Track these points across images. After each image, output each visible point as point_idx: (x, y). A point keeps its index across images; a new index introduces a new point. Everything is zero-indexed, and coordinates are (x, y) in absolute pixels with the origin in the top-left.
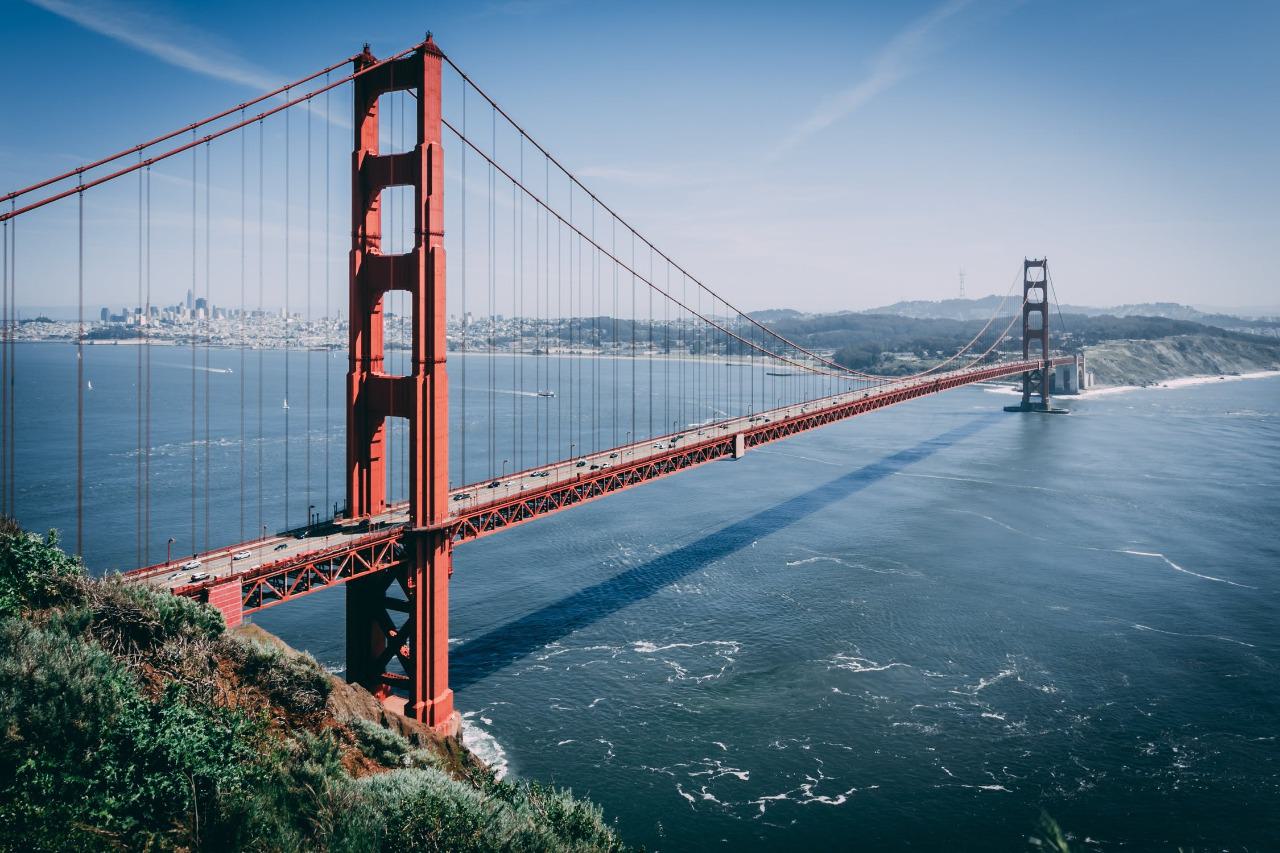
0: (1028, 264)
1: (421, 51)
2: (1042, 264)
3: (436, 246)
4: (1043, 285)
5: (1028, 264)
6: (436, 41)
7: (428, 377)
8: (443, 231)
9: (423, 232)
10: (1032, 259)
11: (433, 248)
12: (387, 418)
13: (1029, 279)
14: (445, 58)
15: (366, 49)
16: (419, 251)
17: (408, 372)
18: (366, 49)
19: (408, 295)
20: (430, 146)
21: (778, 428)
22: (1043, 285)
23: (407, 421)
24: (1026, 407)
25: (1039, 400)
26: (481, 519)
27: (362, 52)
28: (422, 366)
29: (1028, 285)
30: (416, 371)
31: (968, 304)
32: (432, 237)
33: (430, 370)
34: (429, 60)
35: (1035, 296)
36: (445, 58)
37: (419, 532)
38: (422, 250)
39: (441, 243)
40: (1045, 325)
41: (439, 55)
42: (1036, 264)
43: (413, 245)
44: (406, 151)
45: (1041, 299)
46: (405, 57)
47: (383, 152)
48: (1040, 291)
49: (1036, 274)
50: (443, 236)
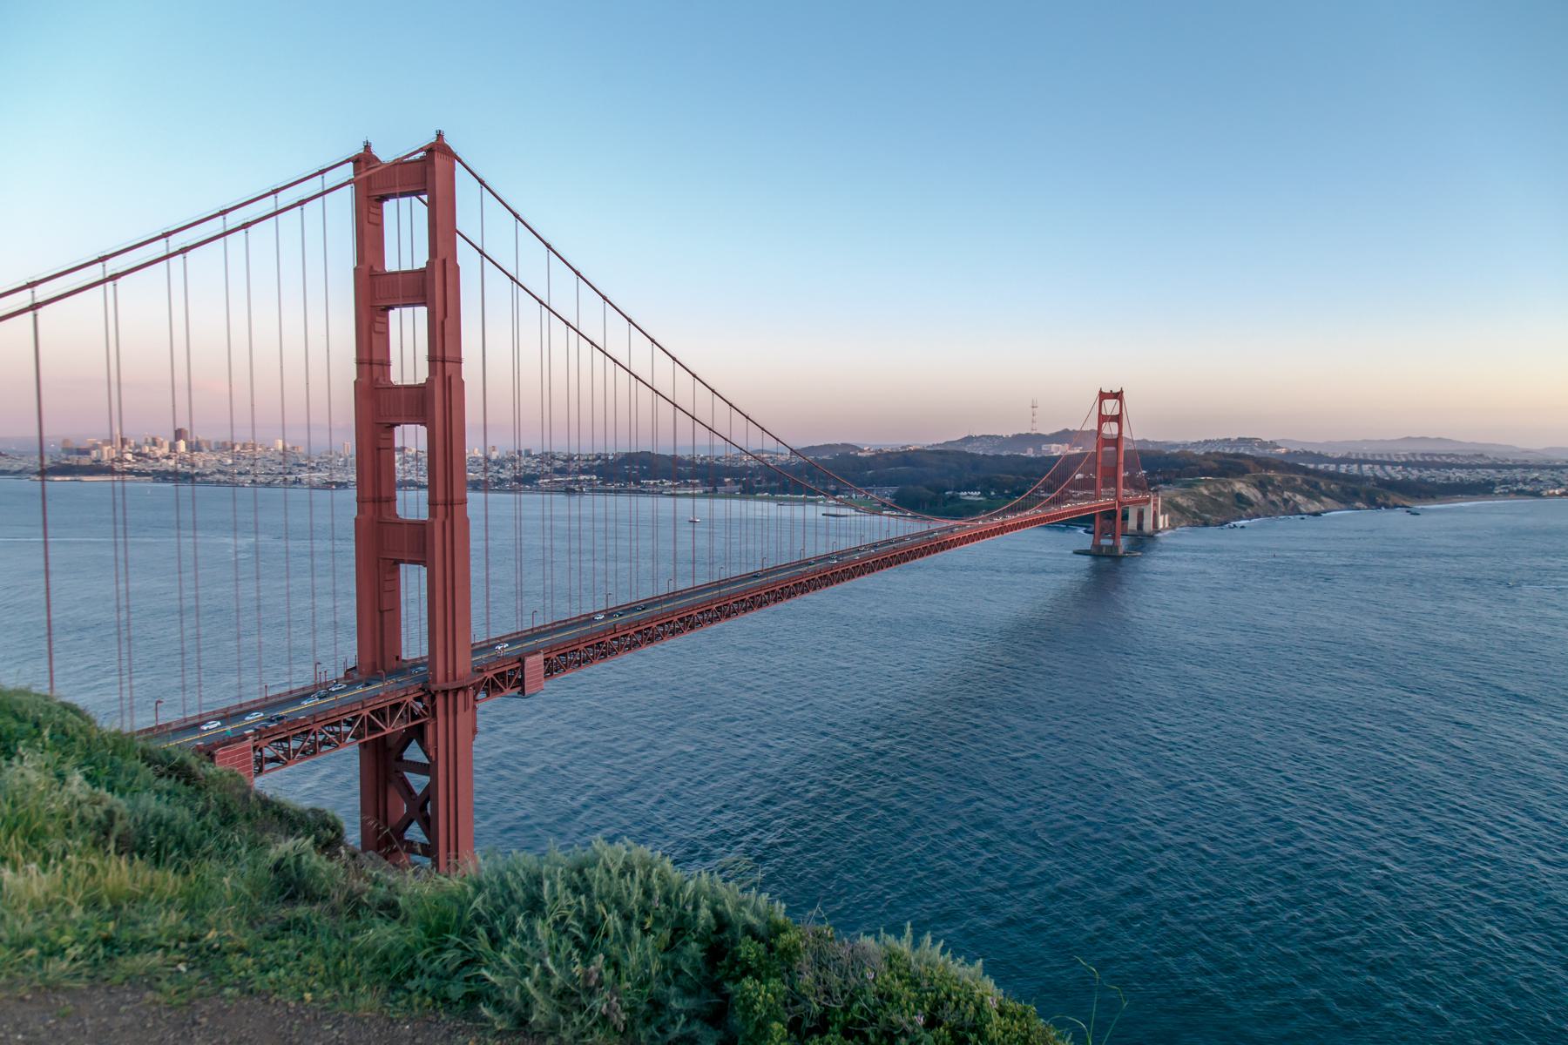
1: (430, 150)
2: (1118, 396)
4: (1117, 419)
5: (1103, 396)
6: (449, 140)
8: (460, 359)
10: (1106, 390)
11: (450, 378)
13: (1103, 413)
14: (460, 161)
16: (433, 381)
17: (424, 515)
20: (444, 261)
21: (832, 574)
22: (1117, 419)
24: (1096, 553)
25: (1110, 542)
27: (362, 151)
29: (1103, 419)
30: (433, 513)
31: (1037, 439)
32: (447, 364)
33: (449, 515)
34: (439, 160)
35: (1110, 429)
36: (460, 161)
37: (436, 692)
40: (1117, 464)
41: (451, 156)
46: (411, 158)
47: (391, 265)
48: (1114, 426)
49: (1110, 407)
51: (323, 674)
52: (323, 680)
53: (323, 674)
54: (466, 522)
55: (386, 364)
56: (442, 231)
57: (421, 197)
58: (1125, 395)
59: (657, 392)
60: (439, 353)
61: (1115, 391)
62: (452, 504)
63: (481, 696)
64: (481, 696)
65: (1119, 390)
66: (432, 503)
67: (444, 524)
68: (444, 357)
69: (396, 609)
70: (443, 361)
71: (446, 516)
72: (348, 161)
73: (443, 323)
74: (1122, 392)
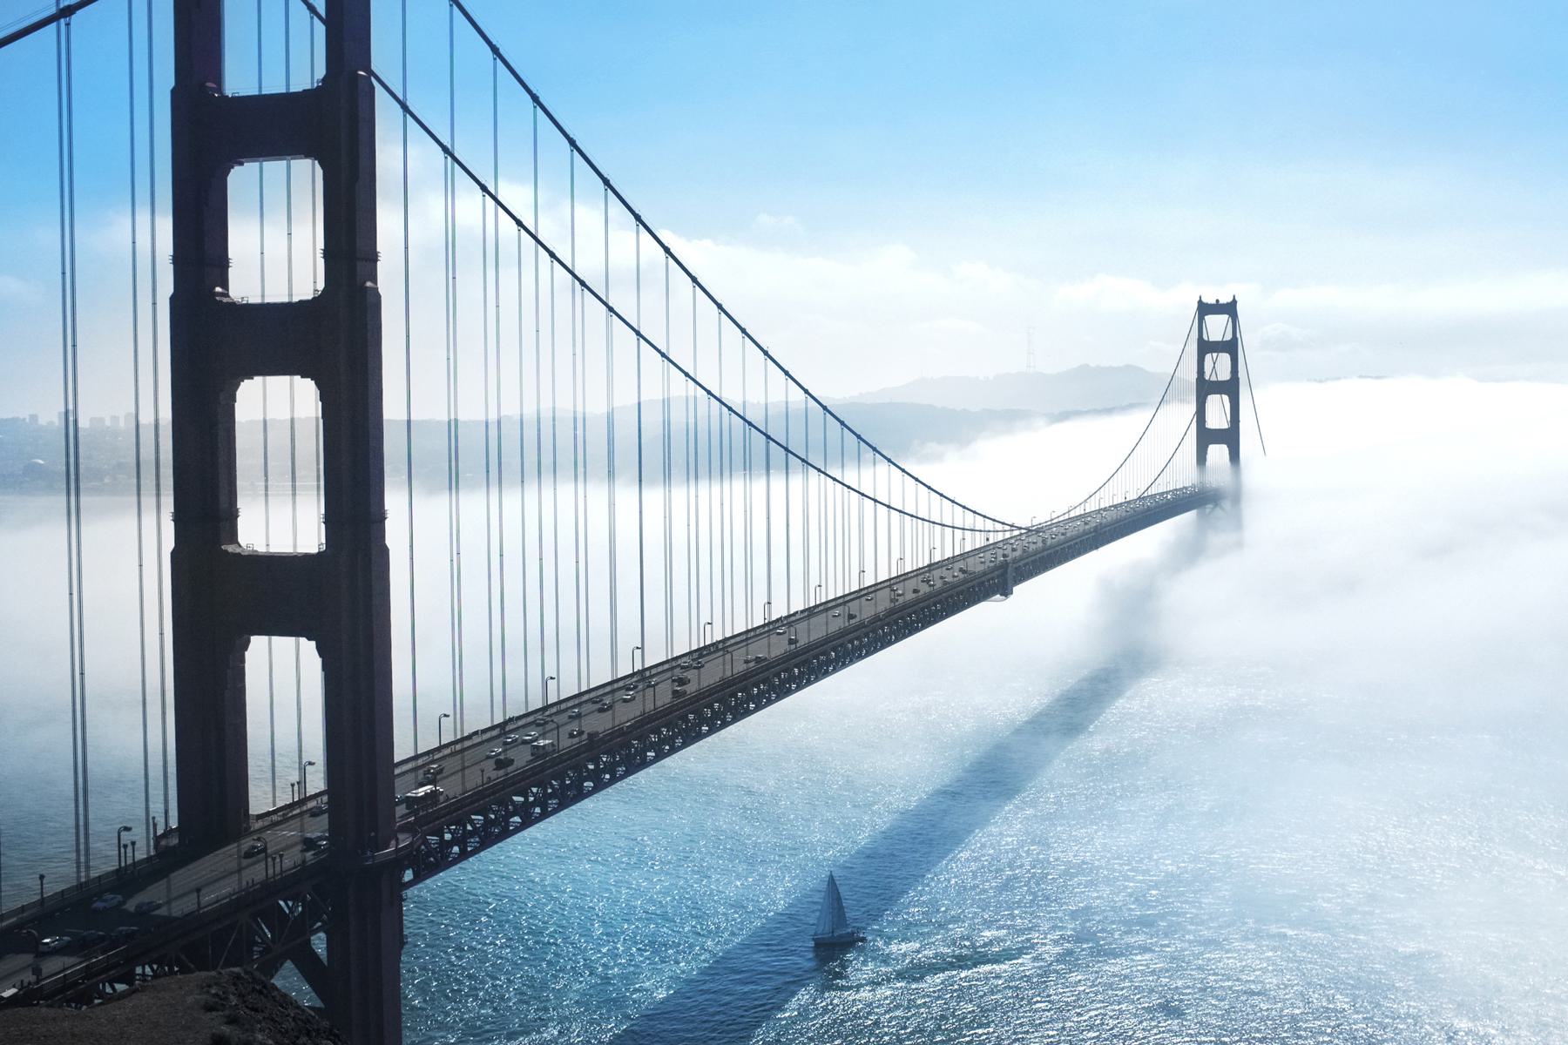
0: (1204, 309)
2: (1230, 309)
3: (369, 284)
5: (1204, 309)
10: (1214, 302)
13: (1206, 339)
22: (1230, 347)
26: (448, 836)
29: (1205, 347)
32: (359, 265)
35: (1219, 367)
39: (373, 277)
42: (1217, 308)
43: (321, 286)
44: (296, 87)
45: (1224, 374)
48: (1225, 358)
49: (1217, 327)
50: (373, 258)
51: (129, 850)
52: (130, 861)
53: (129, 850)
54: (385, 552)
55: (223, 263)
58: (1240, 309)
59: (611, 309)
61: (1223, 301)
63: (408, 875)
64: (408, 875)
65: (1230, 300)
66: (332, 519)
74: (1236, 302)
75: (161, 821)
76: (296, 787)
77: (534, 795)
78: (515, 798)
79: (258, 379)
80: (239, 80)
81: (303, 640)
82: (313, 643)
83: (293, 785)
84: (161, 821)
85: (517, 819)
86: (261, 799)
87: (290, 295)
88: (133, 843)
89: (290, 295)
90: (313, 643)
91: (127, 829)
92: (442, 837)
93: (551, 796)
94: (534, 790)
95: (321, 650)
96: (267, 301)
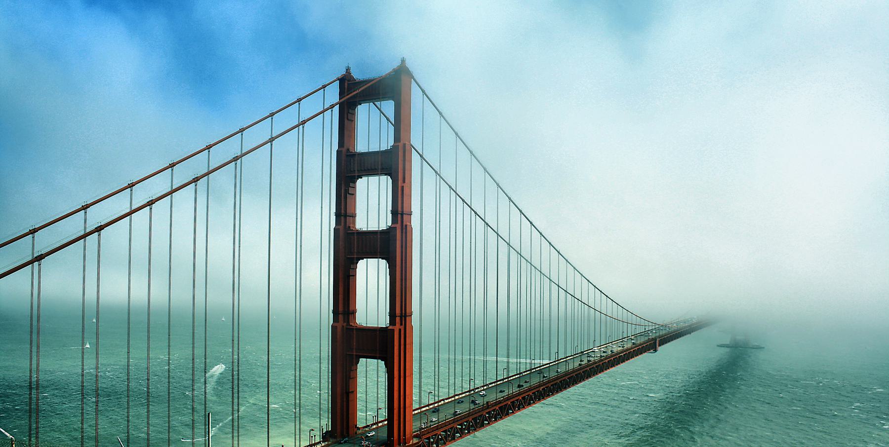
3: (408, 224)
6: (409, 64)
7: (402, 328)
9: (400, 212)
11: (406, 226)
12: (360, 359)
15: (348, 70)
18: (348, 70)
19: (384, 261)
20: (405, 144)
23: (382, 363)
28: (398, 319)
32: (404, 215)
34: (404, 78)
38: (398, 226)
43: (390, 224)
50: (411, 214)
51: (313, 438)
52: (313, 442)
53: (313, 438)
55: (354, 216)
56: (400, 124)
57: (376, 103)
60: (400, 209)
62: (405, 316)
67: (400, 330)
68: (403, 211)
69: (354, 392)
70: (402, 214)
71: (401, 325)
72: (338, 79)
73: (403, 187)
75: (324, 427)
76: (374, 417)
77: (465, 425)
78: (458, 426)
79: (365, 260)
80: (362, 146)
81: (380, 361)
82: (383, 362)
83: (373, 417)
84: (324, 427)
85: (458, 435)
86: (360, 424)
87: (379, 228)
88: (315, 436)
89: (379, 228)
90: (383, 362)
91: (312, 430)
92: (430, 440)
93: (472, 426)
94: (465, 424)
95: (386, 364)
96: (369, 230)
